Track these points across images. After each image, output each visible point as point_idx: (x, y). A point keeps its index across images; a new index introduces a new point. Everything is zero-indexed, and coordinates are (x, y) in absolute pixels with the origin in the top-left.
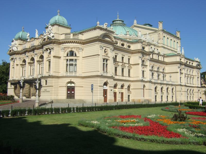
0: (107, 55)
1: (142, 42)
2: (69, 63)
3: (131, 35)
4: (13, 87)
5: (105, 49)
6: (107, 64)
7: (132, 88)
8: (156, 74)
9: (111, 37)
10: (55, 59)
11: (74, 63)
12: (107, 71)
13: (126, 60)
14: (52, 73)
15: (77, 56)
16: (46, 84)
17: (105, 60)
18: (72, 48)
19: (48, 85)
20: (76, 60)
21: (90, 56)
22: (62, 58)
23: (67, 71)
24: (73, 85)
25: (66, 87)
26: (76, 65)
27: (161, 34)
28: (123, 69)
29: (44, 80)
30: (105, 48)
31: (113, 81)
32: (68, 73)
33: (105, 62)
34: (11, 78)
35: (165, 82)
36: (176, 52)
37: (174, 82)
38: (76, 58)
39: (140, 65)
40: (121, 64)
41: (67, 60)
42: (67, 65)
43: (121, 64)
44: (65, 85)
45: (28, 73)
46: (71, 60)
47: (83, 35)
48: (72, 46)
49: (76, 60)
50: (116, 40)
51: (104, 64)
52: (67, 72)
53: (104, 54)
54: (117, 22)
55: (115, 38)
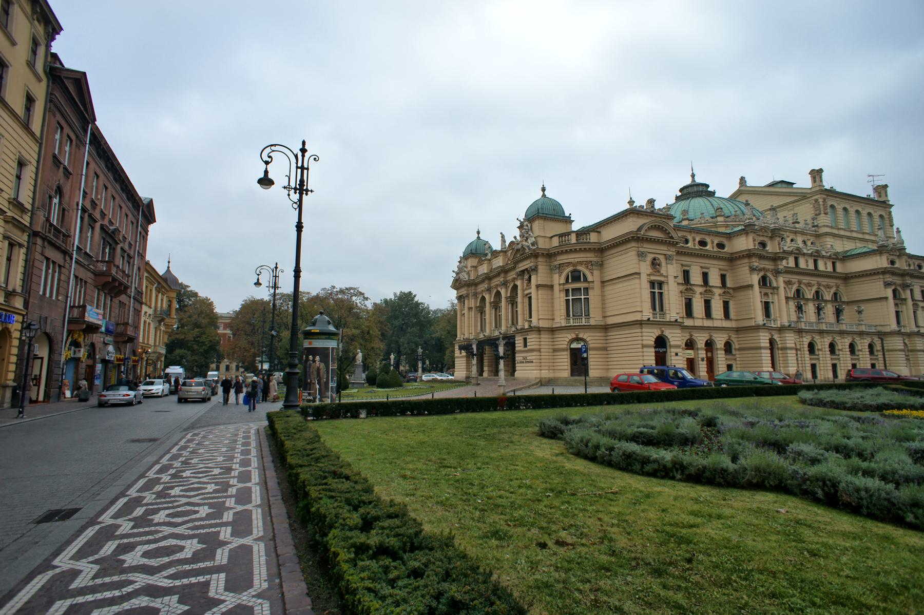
0: (659, 272)
1: (754, 231)
2: (570, 298)
3: (728, 217)
4: (464, 353)
5: (654, 259)
6: (661, 294)
7: (737, 347)
8: (810, 308)
11: (583, 297)
12: (662, 309)
13: (714, 280)
14: (535, 322)
15: (590, 278)
16: (525, 346)
17: (657, 286)
18: (574, 265)
19: (529, 347)
20: (586, 289)
21: (619, 278)
22: (556, 288)
23: (568, 315)
26: (587, 300)
27: (821, 201)
28: (707, 304)
29: (521, 338)
30: (653, 256)
31: (679, 331)
33: (657, 291)
34: (459, 337)
35: (844, 327)
36: (873, 242)
37: (871, 326)
38: (586, 285)
39: (756, 287)
40: (702, 290)
41: (567, 291)
42: (567, 301)
43: (702, 290)
45: (491, 326)
46: (576, 291)
47: (599, 232)
48: (577, 260)
49: (586, 289)
50: (680, 234)
51: (653, 294)
53: (650, 271)
54: (690, 190)
55: (677, 228)
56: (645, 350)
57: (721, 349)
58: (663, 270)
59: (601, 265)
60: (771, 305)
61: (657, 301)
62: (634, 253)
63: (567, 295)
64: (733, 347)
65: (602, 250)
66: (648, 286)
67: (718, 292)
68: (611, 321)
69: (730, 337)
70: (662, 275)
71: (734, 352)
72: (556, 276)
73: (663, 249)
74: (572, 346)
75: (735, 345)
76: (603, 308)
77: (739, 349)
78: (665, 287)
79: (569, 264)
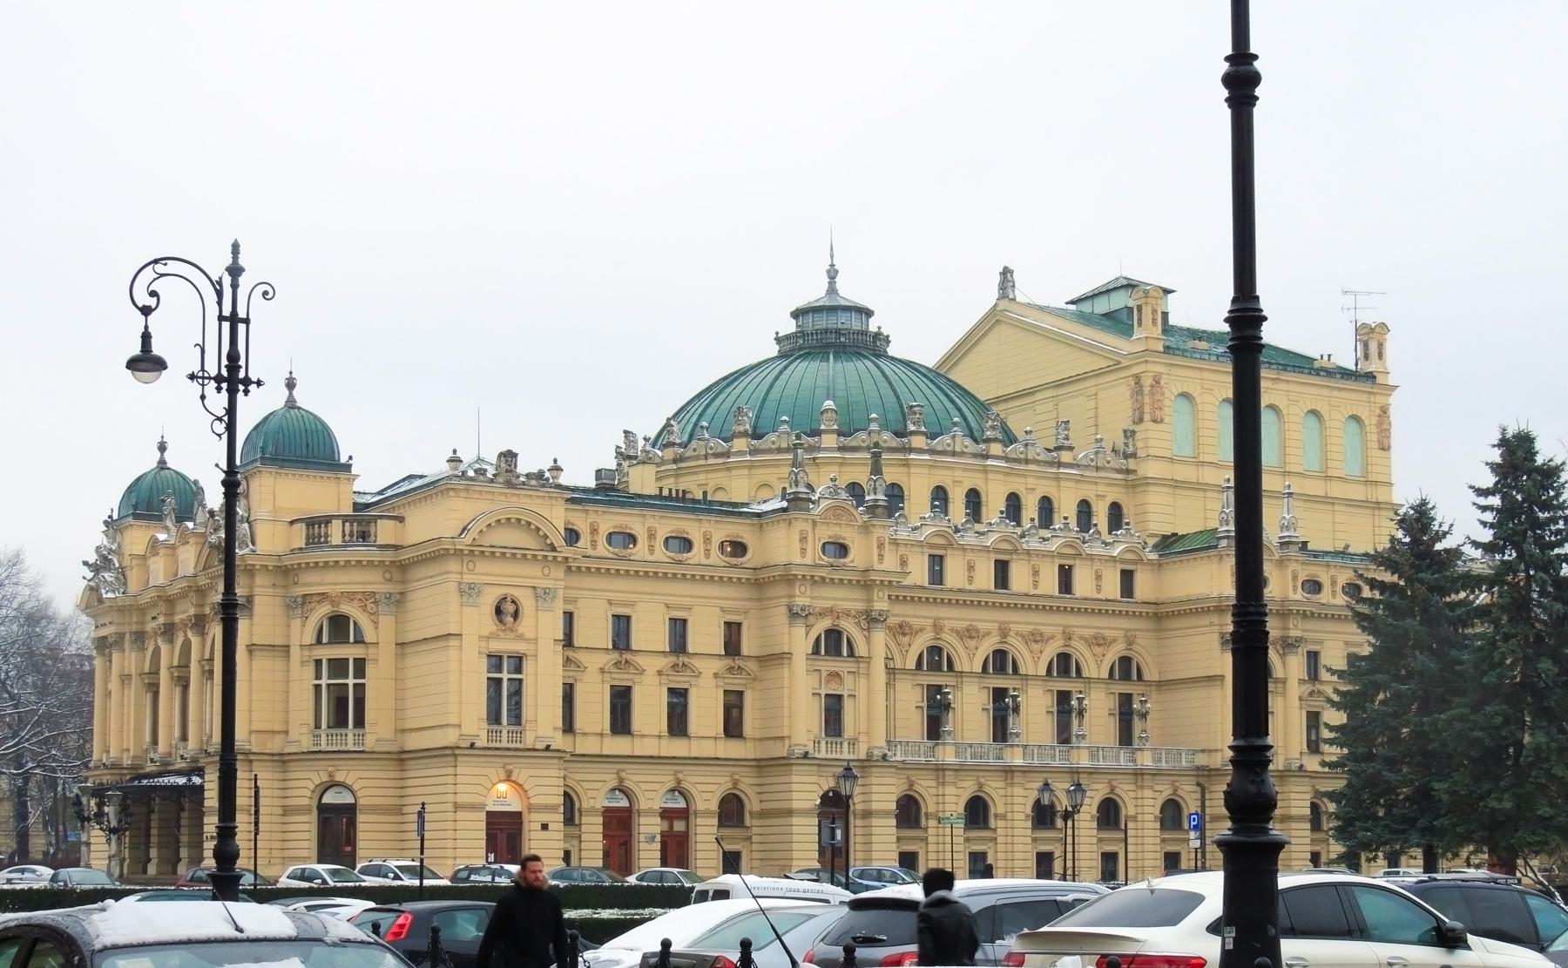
2: (324, 682)
7: (756, 807)
9: (538, 529)
10: (262, 663)
11: (351, 681)
12: (516, 718)
15: (369, 636)
20: (360, 666)
22: (295, 652)
23: (318, 726)
24: (347, 799)
25: (315, 812)
26: (360, 688)
32: (324, 737)
33: (505, 676)
44: (305, 801)
46: (338, 667)
47: (401, 519)
48: (340, 588)
51: (495, 684)
52: (317, 732)
56: (460, 815)
57: (707, 813)
58: (526, 625)
59: (398, 601)
60: (848, 705)
61: (505, 701)
62: (452, 586)
63: (318, 676)
64: (747, 807)
65: (404, 566)
66: (484, 664)
67: (708, 668)
68: (415, 742)
69: (735, 783)
70: (520, 638)
71: (748, 822)
72: (296, 623)
73: (532, 574)
74: (325, 800)
75: (752, 804)
76: (399, 711)
77: (763, 814)
78: (528, 666)
79: (323, 597)
